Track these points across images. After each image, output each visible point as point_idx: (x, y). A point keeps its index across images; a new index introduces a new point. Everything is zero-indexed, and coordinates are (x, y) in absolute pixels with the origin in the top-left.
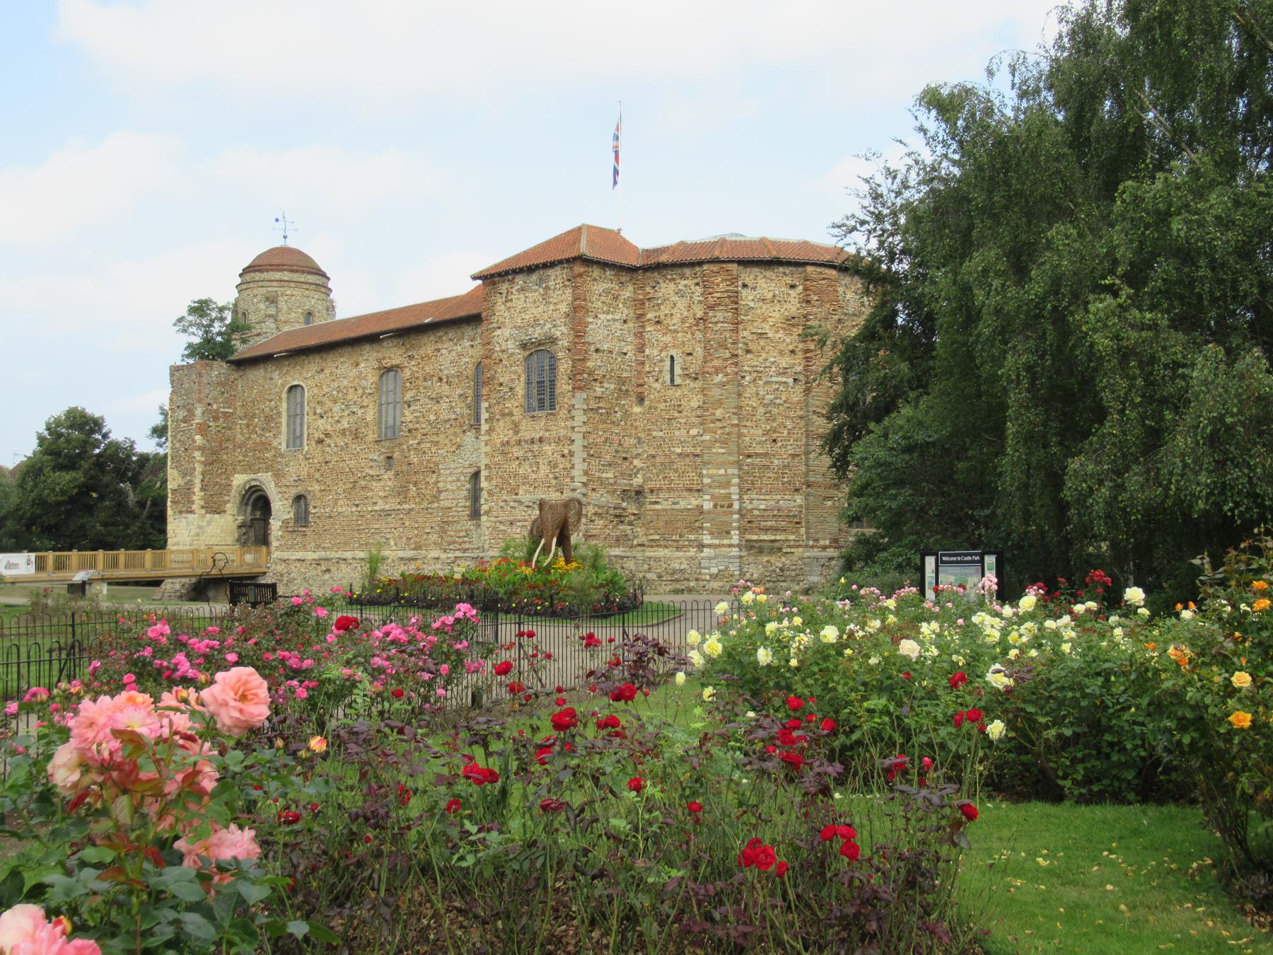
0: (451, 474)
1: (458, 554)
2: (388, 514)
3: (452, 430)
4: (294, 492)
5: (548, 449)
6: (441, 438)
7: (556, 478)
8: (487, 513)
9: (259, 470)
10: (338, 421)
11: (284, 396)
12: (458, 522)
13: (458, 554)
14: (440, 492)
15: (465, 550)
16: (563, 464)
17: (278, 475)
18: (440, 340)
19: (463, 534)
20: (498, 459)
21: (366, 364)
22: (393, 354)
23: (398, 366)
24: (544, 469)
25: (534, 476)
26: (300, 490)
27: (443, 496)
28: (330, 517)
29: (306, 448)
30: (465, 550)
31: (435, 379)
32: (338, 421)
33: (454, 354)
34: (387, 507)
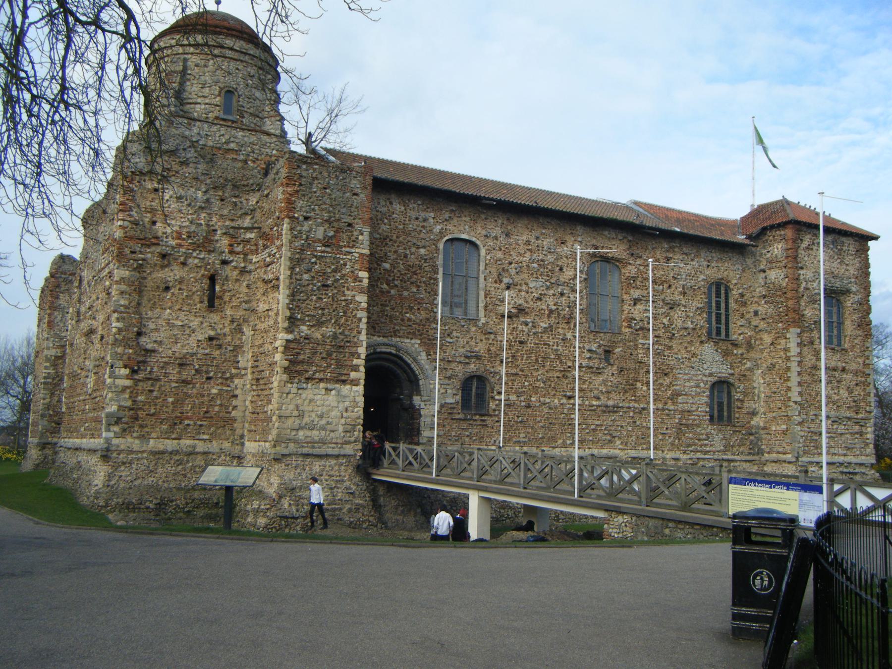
0: (689, 380)
1: (699, 455)
2: (615, 409)
3: (688, 339)
4: (460, 371)
5: (848, 377)
6: (674, 344)
7: (855, 401)
8: (800, 423)
9: (395, 333)
10: (539, 299)
11: (441, 246)
12: (698, 426)
13: (699, 455)
14: (679, 395)
15: (706, 452)
16: (858, 391)
17: (429, 344)
18: (671, 249)
19: (704, 437)
20: (806, 378)
21: (578, 249)
22: (615, 248)
23: (618, 260)
24: (844, 393)
25: (836, 398)
26: (472, 367)
27: (680, 399)
28: (528, 406)
29: (483, 320)
30: (706, 452)
31: (666, 285)
32: (539, 299)
33: (694, 269)
34: (610, 403)
